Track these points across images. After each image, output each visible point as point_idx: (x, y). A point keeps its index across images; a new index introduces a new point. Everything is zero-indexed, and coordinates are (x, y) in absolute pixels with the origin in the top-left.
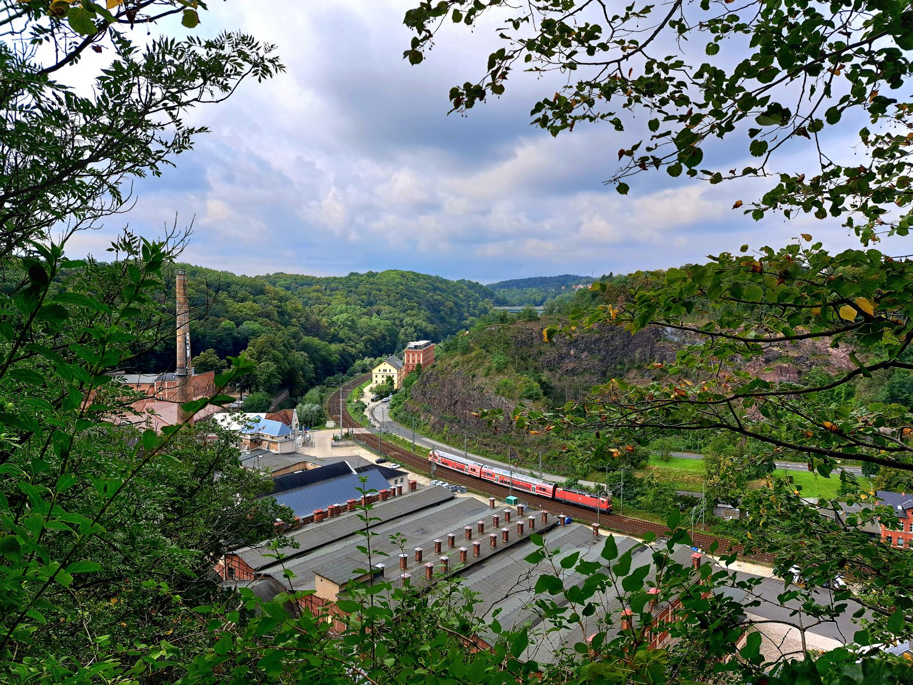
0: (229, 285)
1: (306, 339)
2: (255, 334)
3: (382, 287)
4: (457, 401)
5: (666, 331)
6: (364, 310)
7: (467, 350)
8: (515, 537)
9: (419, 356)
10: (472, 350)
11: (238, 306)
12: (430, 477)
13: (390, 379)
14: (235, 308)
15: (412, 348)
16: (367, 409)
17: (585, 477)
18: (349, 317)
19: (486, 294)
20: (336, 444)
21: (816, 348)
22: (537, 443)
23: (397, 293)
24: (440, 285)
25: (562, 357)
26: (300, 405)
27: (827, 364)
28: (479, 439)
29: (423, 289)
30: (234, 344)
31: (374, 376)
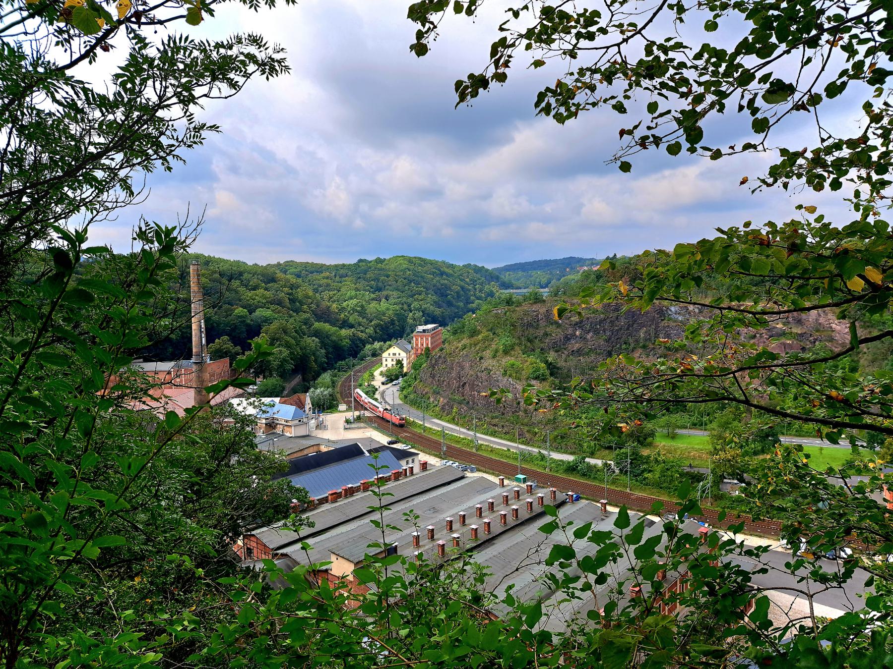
0: (241, 274)
1: (317, 325)
2: (268, 321)
3: (390, 273)
4: (465, 383)
5: (671, 310)
6: (373, 296)
7: (474, 333)
8: (524, 515)
9: (427, 339)
10: (480, 332)
11: (250, 294)
12: (441, 458)
13: (399, 362)
14: (247, 296)
15: (421, 332)
16: (377, 392)
17: (592, 455)
18: (358, 303)
19: (492, 278)
20: (348, 426)
21: (820, 324)
24: (446, 270)
25: (567, 338)
26: (312, 390)
27: (831, 340)
29: (430, 274)
30: (247, 331)
31: (384, 360)
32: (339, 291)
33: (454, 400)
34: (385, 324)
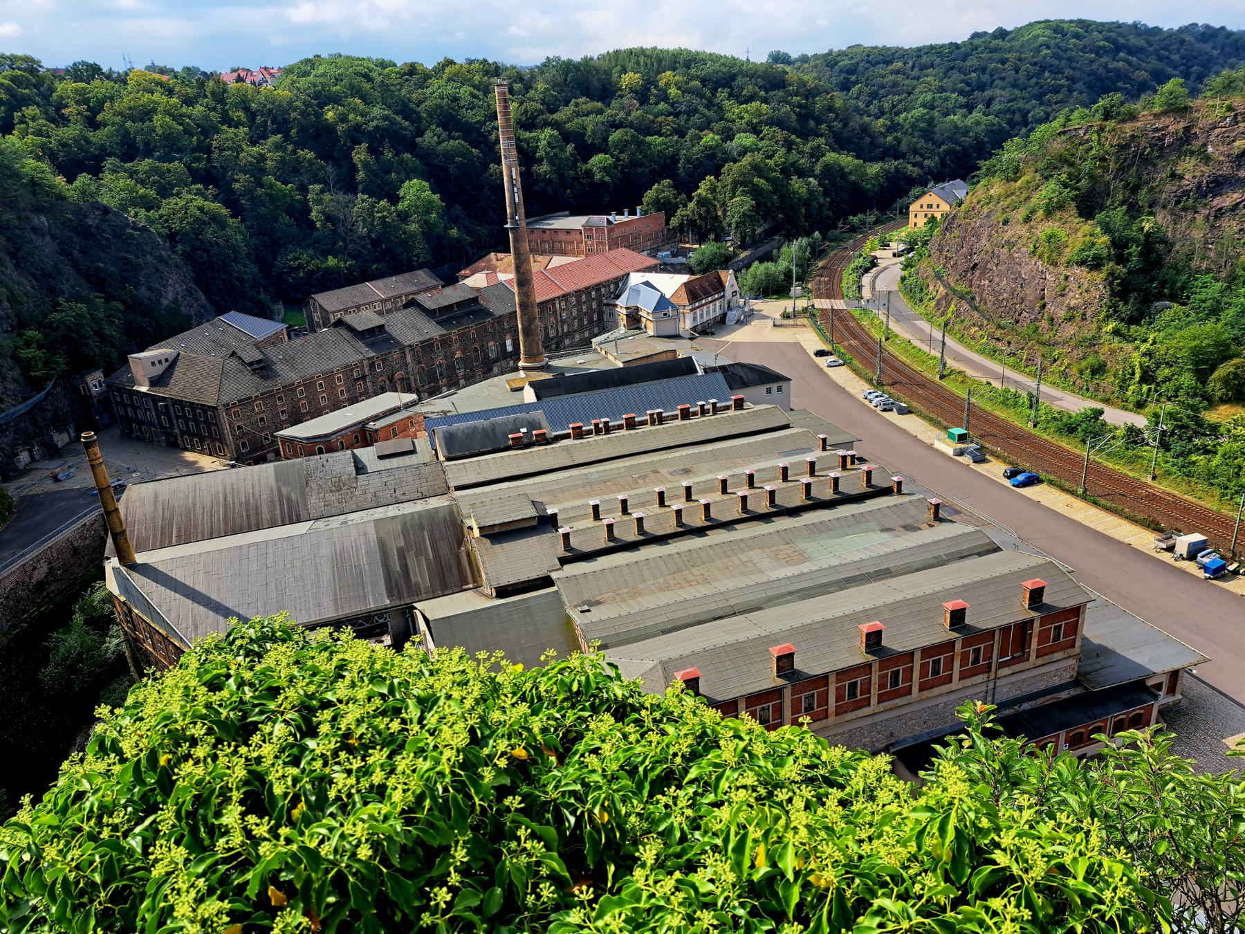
0: (733, 77)
1: (831, 157)
4: (976, 265)
6: (962, 100)
8: (799, 499)
18: (924, 115)
22: (1073, 343)
23: (1035, 64)
28: (991, 328)
29: (1092, 51)
31: (912, 215)
32: (910, 94)
33: (955, 291)
34: (964, 149)
